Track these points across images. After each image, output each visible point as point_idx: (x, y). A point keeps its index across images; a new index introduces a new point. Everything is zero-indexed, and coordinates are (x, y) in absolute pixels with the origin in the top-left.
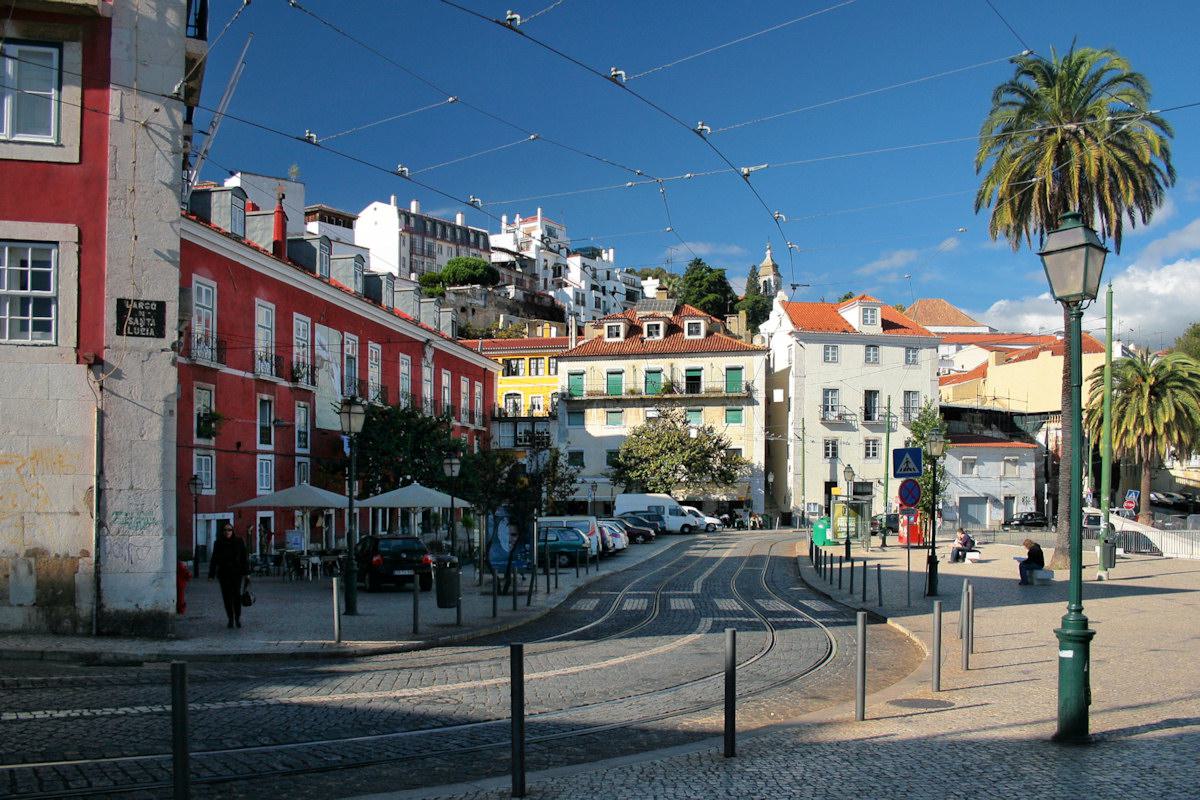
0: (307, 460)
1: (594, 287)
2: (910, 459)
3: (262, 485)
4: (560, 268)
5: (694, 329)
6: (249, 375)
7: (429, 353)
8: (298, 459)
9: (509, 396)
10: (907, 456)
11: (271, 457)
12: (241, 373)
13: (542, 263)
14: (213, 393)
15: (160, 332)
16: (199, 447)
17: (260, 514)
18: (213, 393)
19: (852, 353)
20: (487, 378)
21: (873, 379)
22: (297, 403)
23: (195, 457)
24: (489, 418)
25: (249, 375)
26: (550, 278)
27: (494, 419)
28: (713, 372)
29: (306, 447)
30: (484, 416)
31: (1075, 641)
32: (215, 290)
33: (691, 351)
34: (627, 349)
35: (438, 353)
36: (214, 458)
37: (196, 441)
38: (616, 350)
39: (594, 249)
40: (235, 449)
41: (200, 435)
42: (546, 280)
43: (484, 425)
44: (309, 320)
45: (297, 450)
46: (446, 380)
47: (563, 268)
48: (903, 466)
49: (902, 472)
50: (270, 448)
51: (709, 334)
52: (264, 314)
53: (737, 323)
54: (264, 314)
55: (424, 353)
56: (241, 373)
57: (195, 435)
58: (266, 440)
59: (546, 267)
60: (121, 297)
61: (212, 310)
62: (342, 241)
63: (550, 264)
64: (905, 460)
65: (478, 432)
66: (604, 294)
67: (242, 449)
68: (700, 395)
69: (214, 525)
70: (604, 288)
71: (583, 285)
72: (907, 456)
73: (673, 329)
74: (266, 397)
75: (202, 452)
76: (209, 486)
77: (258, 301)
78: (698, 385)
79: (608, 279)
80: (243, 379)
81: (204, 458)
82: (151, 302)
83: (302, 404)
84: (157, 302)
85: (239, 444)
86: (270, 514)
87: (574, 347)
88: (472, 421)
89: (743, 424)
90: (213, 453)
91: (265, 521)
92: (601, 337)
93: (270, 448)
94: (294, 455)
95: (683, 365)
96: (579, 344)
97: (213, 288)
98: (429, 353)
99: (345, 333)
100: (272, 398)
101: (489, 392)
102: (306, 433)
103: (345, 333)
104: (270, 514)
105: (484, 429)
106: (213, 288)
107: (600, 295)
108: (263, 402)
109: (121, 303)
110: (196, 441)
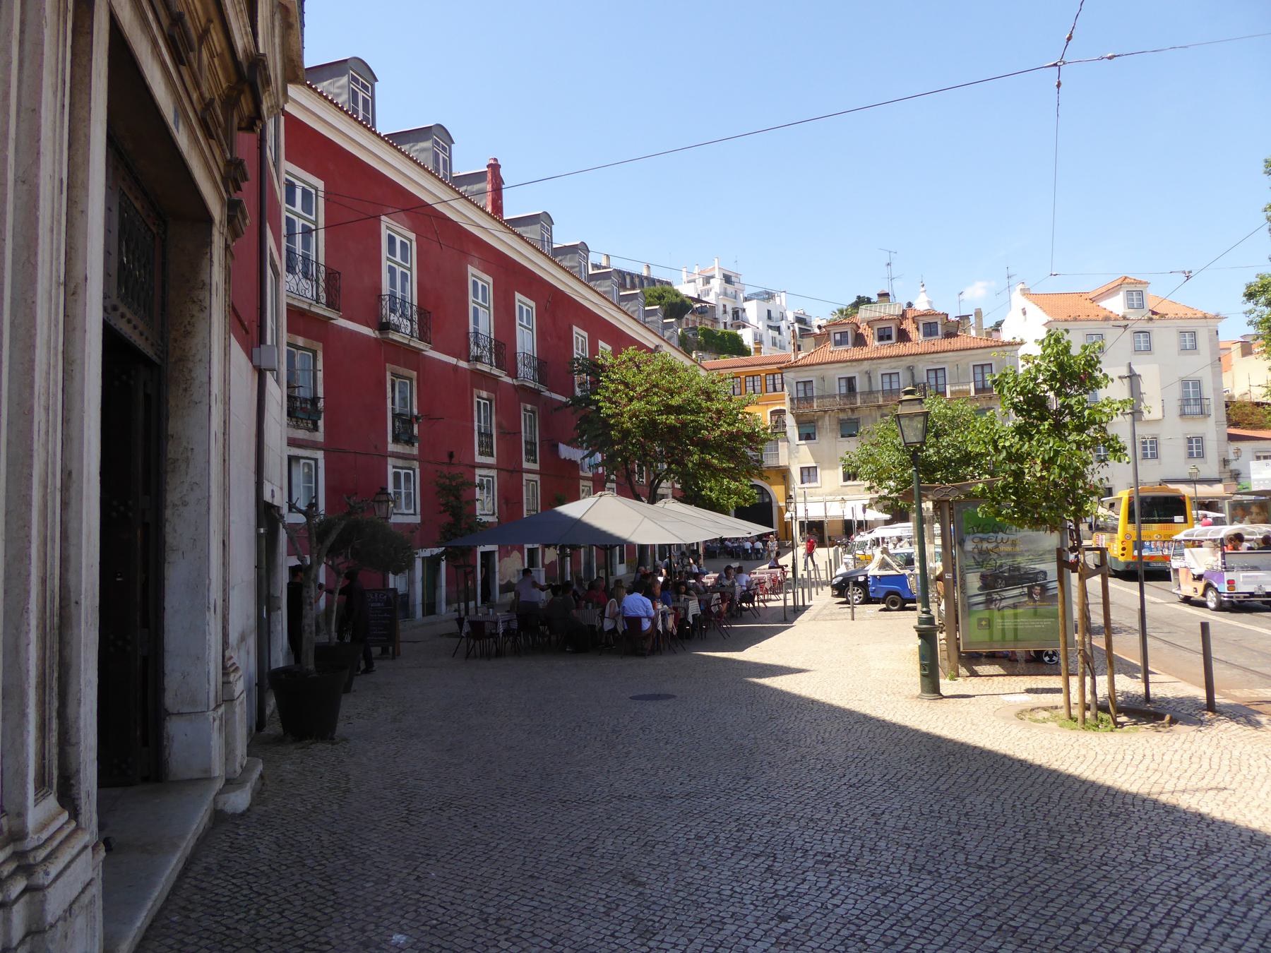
0: (537, 477)
6: (463, 364)
8: (525, 476)
11: (494, 473)
12: (453, 360)
13: (721, 308)
16: (396, 455)
18: (415, 383)
22: (522, 405)
23: (390, 471)
25: (463, 364)
26: (729, 319)
29: (535, 461)
32: (414, 244)
36: (418, 471)
37: (392, 447)
39: (768, 293)
40: (447, 460)
41: (396, 439)
45: (526, 465)
50: (491, 460)
56: (453, 360)
57: (390, 439)
58: (486, 450)
59: (725, 312)
61: (410, 269)
63: (729, 309)
71: (760, 325)
75: (400, 463)
76: (412, 511)
77: (471, 270)
80: (456, 367)
81: (403, 472)
83: (529, 407)
85: (451, 455)
90: (416, 464)
93: (491, 460)
94: (521, 471)
97: (411, 241)
100: (493, 396)
106: (411, 241)
110: (392, 447)
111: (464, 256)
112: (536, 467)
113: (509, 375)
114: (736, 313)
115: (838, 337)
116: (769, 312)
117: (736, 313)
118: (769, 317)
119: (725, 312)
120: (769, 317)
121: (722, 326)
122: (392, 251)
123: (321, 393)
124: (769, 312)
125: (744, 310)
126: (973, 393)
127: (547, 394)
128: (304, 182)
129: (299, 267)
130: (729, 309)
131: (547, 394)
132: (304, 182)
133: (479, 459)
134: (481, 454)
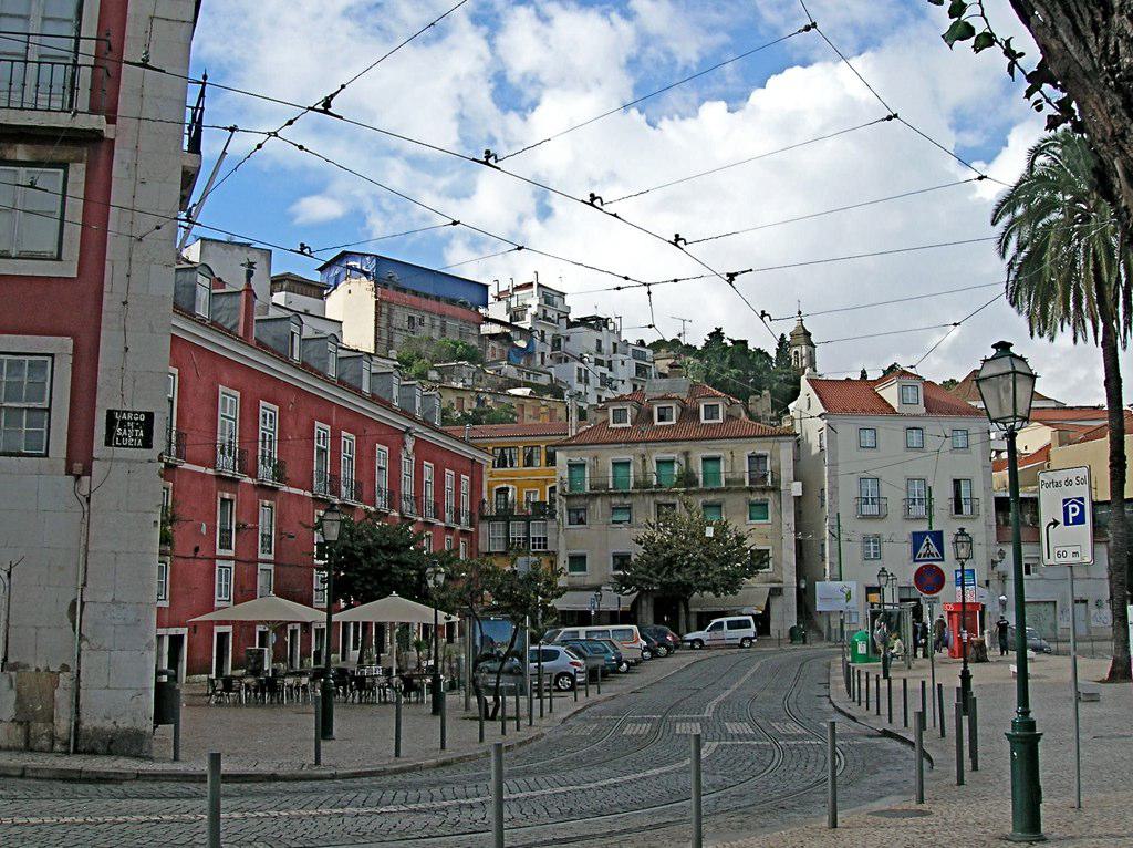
1: (599, 362)
3: (220, 596)
4: (559, 340)
5: (711, 411)
6: (210, 471)
7: (410, 443)
14: (171, 492)
15: (147, 443)
17: (218, 629)
19: (891, 434)
20: (475, 468)
21: (919, 466)
24: (477, 514)
26: (548, 351)
27: (483, 518)
28: (735, 460)
29: (270, 552)
30: (472, 514)
31: (1023, 743)
33: (712, 435)
34: (633, 438)
39: (597, 318)
42: (543, 353)
43: (471, 525)
46: (428, 470)
47: (562, 340)
51: (729, 417)
52: (229, 402)
53: (763, 404)
54: (229, 402)
59: (543, 340)
60: (111, 408)
62: (311, 313)
63: (548, 338)
65: (463, 532)
66: (610, 370)
67: (198, 555)
69: (166, 641)
70: (610, 362)
73: (689, 414)
74: (227, 496)
79: (615, 352)
82: (140, 413)
83: (267, 503)
84: (145, 413)
86: (229, 629)
87: (574, 434)
88: (458, 521)
89: (770, 521)
91: (222, 637)
92: (607, 421)
93: (231, 553)
94: (256, 562)
95: (698, 454)
96: (580, 431)
97: (174, 375)
98: (410, 443)
101: (476, 486)
102: (270, 536)
104: (229, 629)
105: (472, 530)
106: (174, 375)
107: (605, 370)
108: (223, 500)
109: (110, 414)
112: (271, 557)
113: (250, 476)
116: (599, 342)
117: (556, 343)
118: (599, 349)
119: (543, 340)
120: (599, 349)
121: (539, 358)
124: (599, 342)
125: (568, 339)
126: (747, 484)
127: (285, 489)
130: (548, 338)
131: (285, 489)
133: (219, 552)
134: (221, 547)
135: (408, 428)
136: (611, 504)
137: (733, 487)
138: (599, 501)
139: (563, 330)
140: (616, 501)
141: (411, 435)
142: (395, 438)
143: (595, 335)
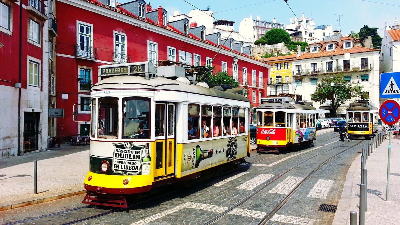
2: (394, 83)
4: (311, 34)
7: (236, 61)
9: (277, 77)
10: (392, 79)
30: (264, 83)
32: (126, 37)
34: (319, 56)
35: (240, 62)
38: (315, 56)
44: (175, 49)
48: (388, 88)
49: (387, 94)
55: (233, 61)
64: (390, 83)
65: (260, 90)
68: (350, 71)
72: (392, 79)
78: (349, 67)
97: (125, 36)
98: (236, 61)
99: (194, 54)
103: (194, 54)
111: (147, 38)
114: (310, 35)
115: (313, 49)
116: (324, 33)
122: (118, 39)
123: (92, 79)
124: (324, 33)
125: (314, 33)
126: (360, 69)
128: (86, 26)
129: (85, 49)
132: (86, 26)
135: (235, 56)
136: (310, 78)
137: (356, 71)
138: (306, 78)
139: (312, 32)
140: (311, 77)
141: (236, 58)
142: (230, 60)
143: (323, 31)
